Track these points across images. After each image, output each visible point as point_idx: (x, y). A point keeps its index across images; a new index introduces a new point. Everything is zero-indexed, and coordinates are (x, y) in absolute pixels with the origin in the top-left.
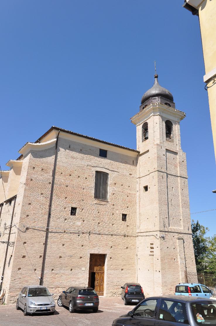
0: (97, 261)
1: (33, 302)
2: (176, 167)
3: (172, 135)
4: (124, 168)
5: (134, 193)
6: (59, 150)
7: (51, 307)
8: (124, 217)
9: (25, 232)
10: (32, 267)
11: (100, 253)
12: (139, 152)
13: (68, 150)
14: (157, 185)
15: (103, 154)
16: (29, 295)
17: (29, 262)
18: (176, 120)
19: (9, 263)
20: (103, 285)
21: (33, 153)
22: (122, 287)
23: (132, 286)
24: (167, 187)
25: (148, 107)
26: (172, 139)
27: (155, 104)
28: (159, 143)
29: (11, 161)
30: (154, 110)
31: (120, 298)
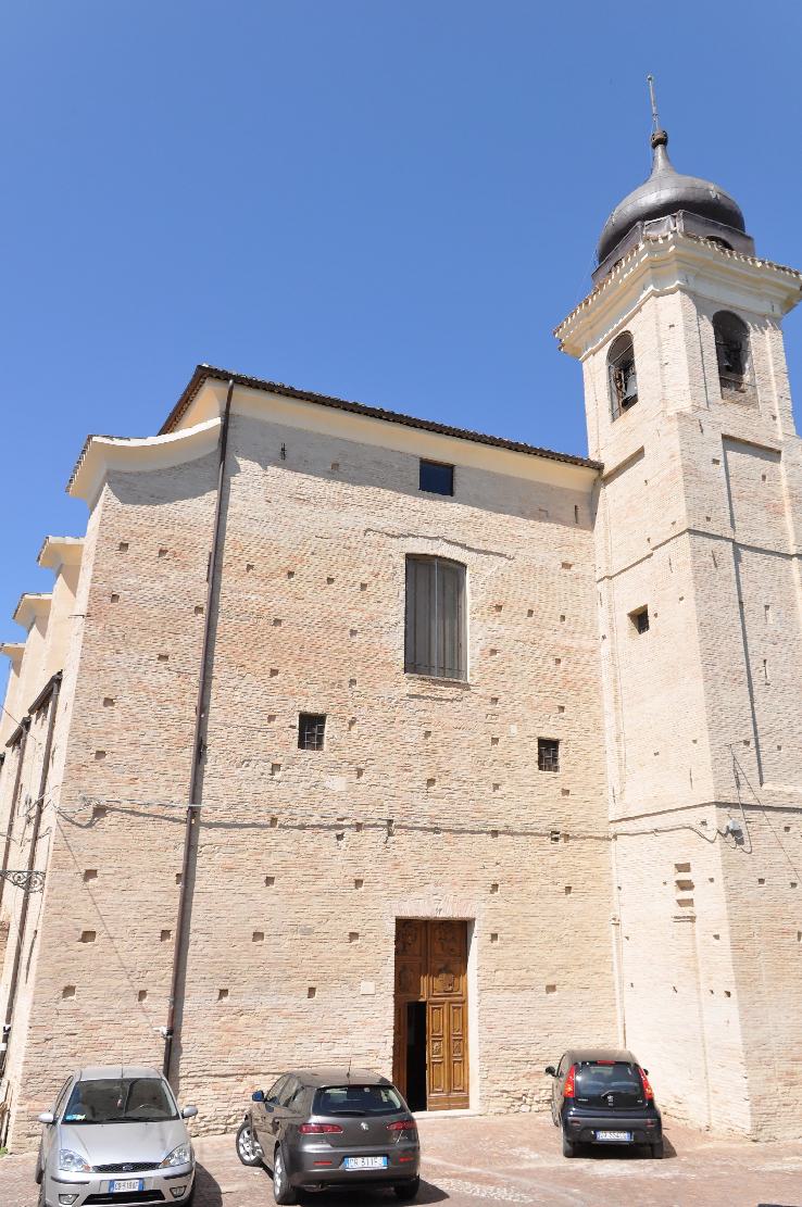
0: (429, 949)
1: (79, 1152)
2: (780, 514)
3: (747, 377)
4: (537, 540)
5: (590, 645)
6: (237, 469)
7: (167, 1178)
8: (548, 751)
9: (90, 825)
10: (126, 982)
11: (442, 915)
12: (599, 467)
13: (279, 466)
14: (689, 591)
15: (437, 480)
16: (69, 1118)
17: (114, 958)
18: (764, 307)
19: (28, 969)
20: (463, 1062)
21: (120, 481)
22: (550, 1071)
23: (594, 1063)
24: (741, 603)
25: (626, 261)
26: (749, 392)
27: (661, 241)
28: (688, 410)
29: (52, 539)
30: (656, 270)
31: (548, 1118)
